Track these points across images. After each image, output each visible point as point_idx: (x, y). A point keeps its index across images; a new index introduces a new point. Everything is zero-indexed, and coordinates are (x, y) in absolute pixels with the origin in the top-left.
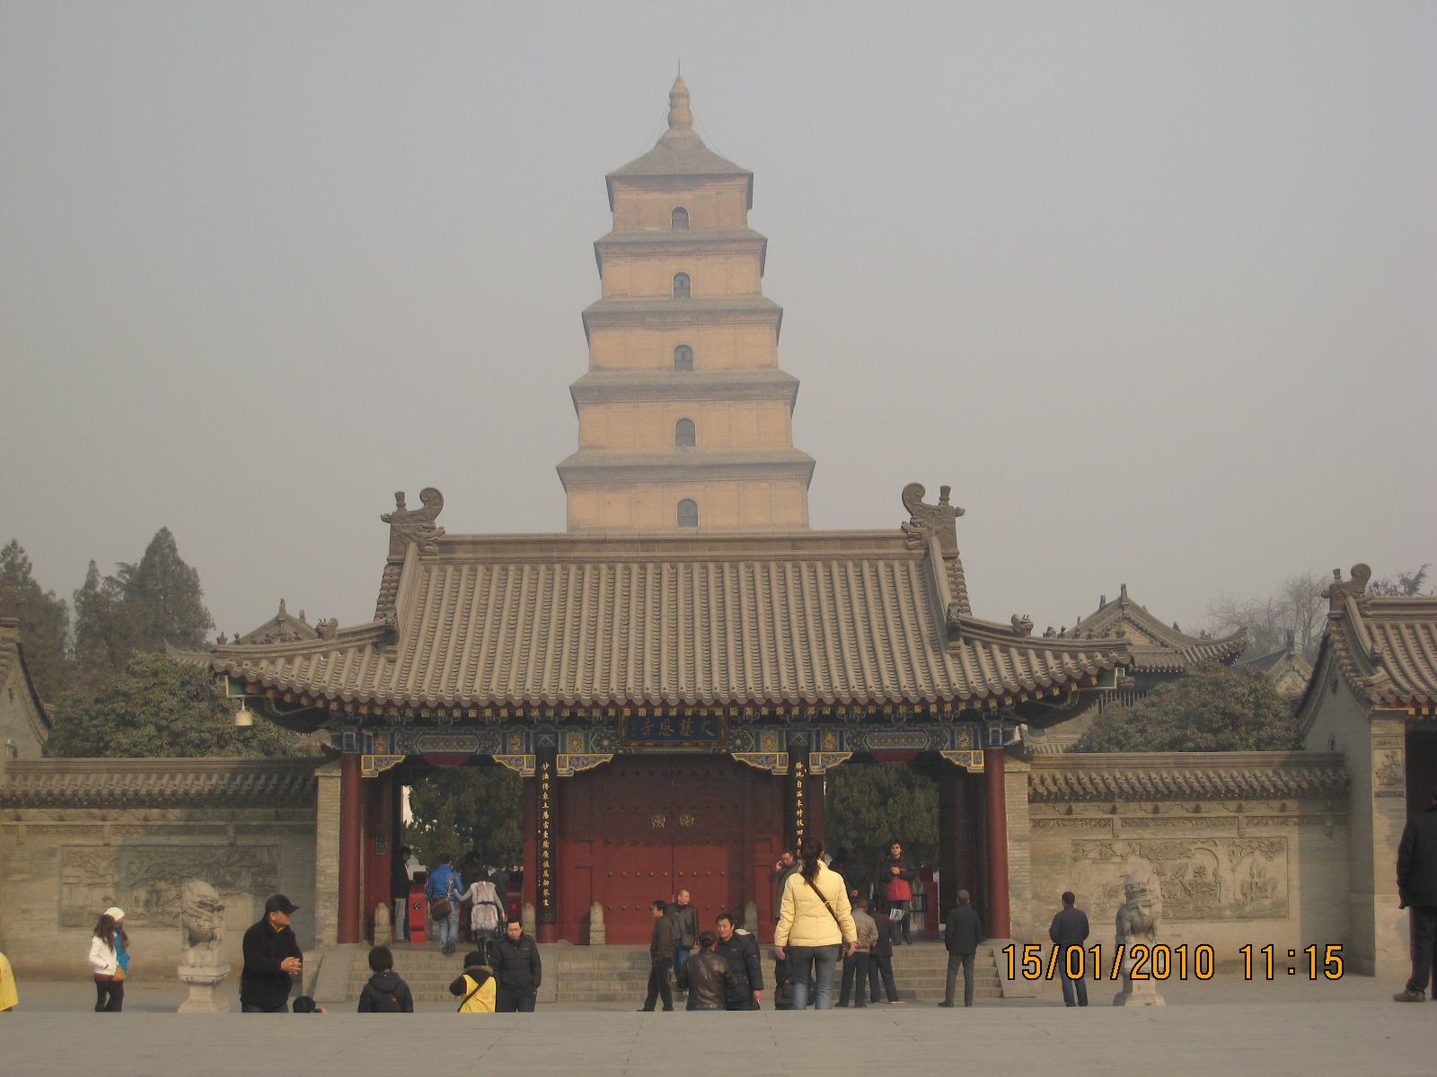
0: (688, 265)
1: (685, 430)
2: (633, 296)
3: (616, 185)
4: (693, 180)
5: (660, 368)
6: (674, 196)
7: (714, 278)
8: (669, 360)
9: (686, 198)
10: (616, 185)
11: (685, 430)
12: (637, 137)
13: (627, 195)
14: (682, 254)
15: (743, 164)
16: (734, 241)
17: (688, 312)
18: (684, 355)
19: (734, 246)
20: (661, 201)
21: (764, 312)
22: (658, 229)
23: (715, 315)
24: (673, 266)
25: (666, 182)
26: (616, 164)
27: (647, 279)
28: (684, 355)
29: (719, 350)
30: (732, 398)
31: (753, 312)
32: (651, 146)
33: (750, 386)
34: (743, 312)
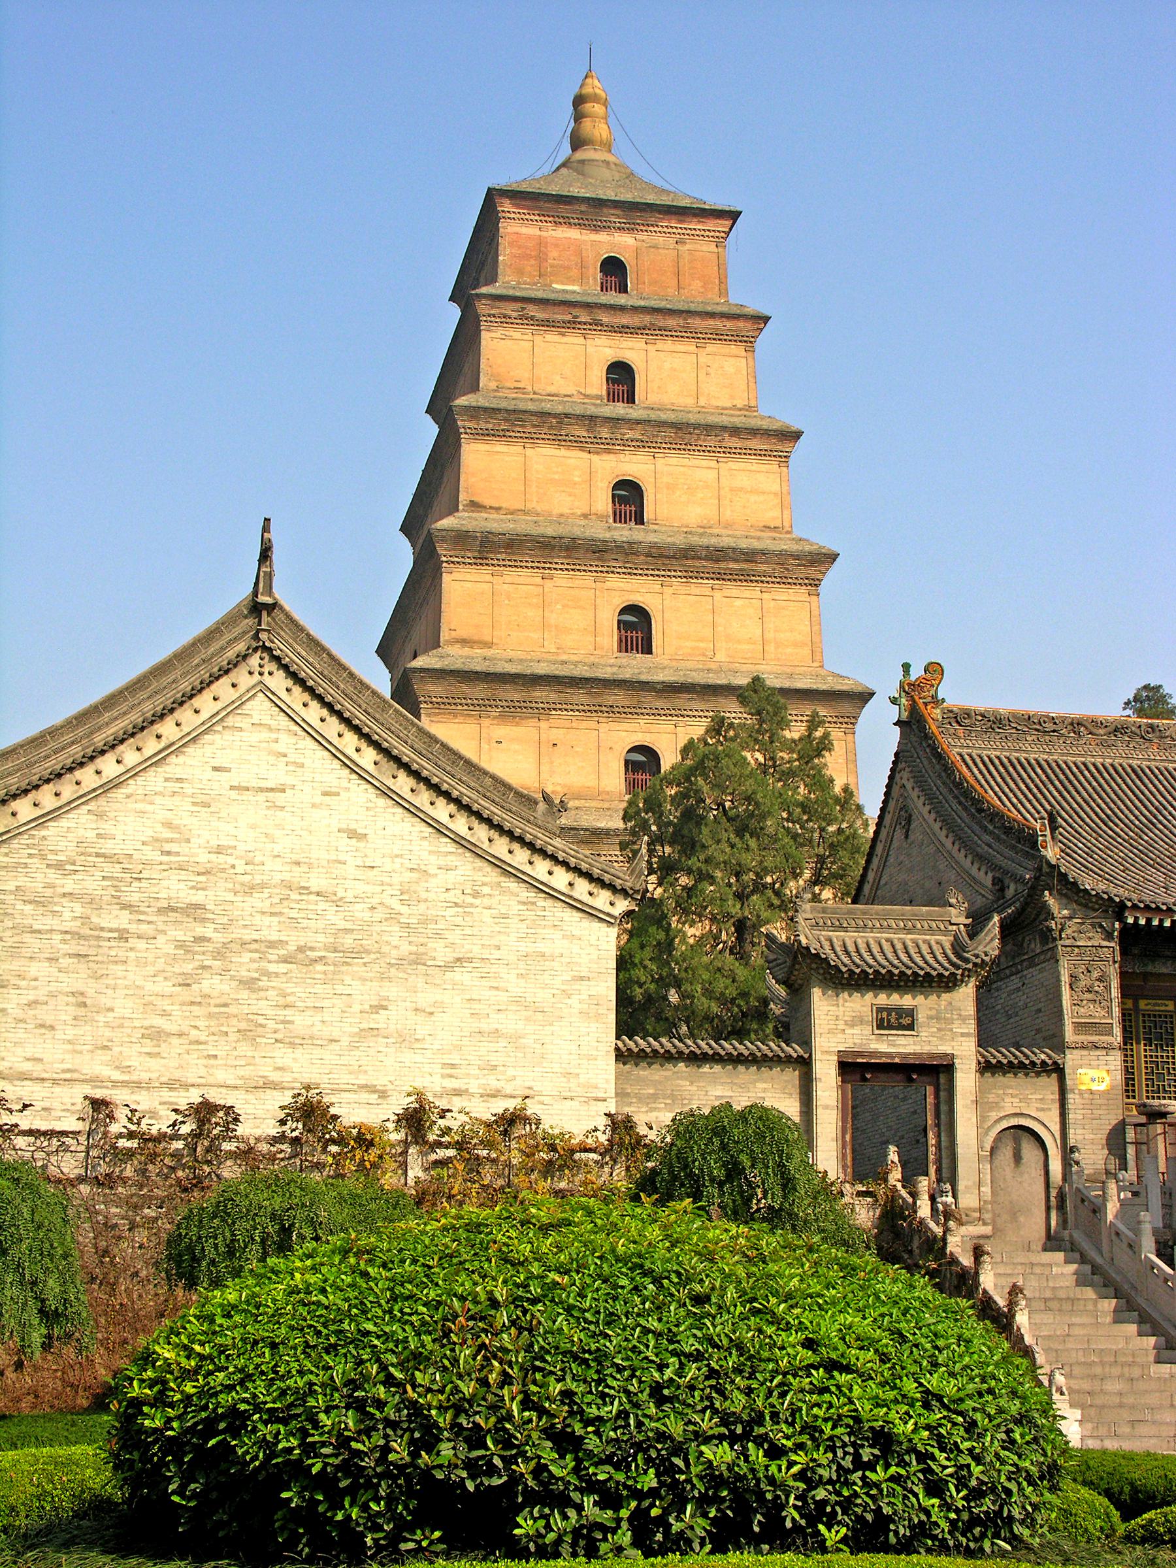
0: (631, 350)
2: (535, 393)
3: (505, 206)
4: (639, 213)
5: (585, 516)
6: (602, 237)
7: (673, 375)
8: (603, 503)
9: (621, 243)
10: (505, 206)
11: (636, 627)
14: (624, 330)
16: (712, 315)
17: (638, 422)
18: (629, 497)
19: (711, 323)
21: (769, 434)
22: (576, 288)
24: (606, 349)
25: (593, 211)
28: (629, 497)
29: (691, 495)
30: (719, 576)
31: (753, 432)
33: (750, 556)
34: (735, 431)
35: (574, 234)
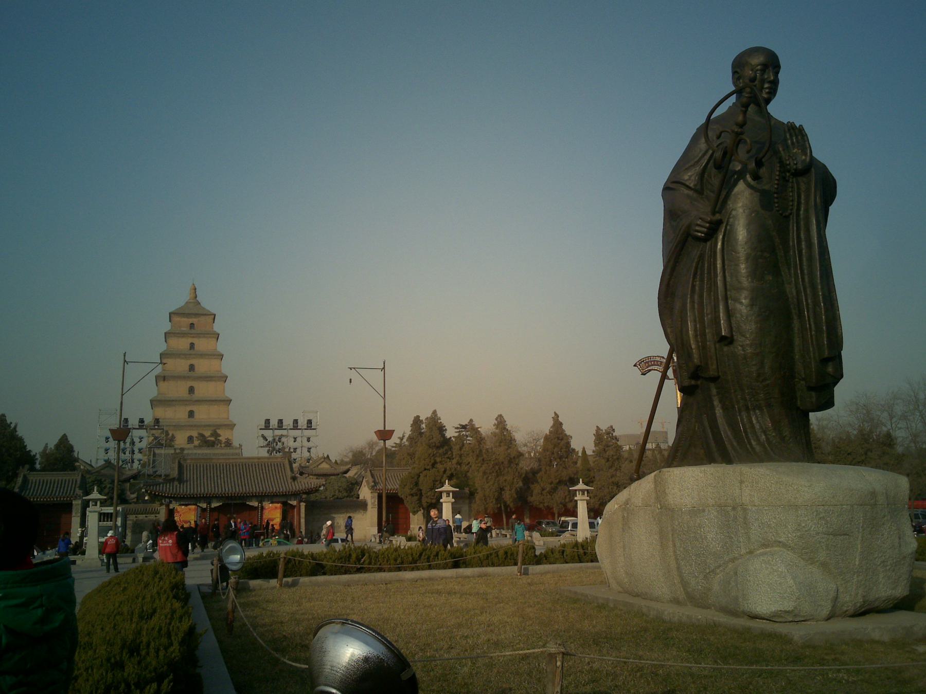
0: (195, 341)
1: (191, 390)
4: (197, 315)
7: (202, 345)
8: (187, 368)
12: (179, 300)
13: (176, 319)
15: (213, 311)
18: (192, 368)
20: (185, 321)
23: (202, 355)
24: (190, 340)
26: (172, 309)
27: (182, 344)
28: (192, 368)
29: (203, 366)
32: (183, 304)
35: (185, 319)
